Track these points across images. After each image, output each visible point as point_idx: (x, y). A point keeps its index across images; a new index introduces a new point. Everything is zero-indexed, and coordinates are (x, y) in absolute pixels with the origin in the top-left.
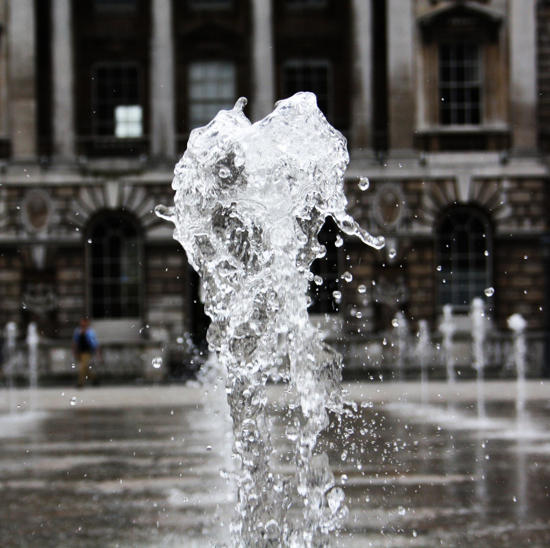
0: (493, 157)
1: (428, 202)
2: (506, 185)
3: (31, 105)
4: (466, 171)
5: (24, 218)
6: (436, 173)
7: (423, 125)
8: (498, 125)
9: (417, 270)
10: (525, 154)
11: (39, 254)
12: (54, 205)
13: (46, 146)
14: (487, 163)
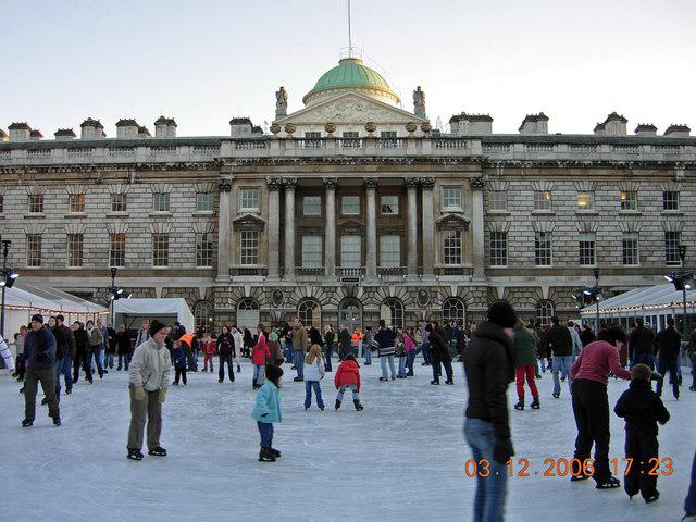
0: (467, 278)
1: (439, 296)
2: (471, 289)
7: (438, 265)
8: (469, 265)
10: (479, 276)
13: (282, 272)
14: (463, 280)
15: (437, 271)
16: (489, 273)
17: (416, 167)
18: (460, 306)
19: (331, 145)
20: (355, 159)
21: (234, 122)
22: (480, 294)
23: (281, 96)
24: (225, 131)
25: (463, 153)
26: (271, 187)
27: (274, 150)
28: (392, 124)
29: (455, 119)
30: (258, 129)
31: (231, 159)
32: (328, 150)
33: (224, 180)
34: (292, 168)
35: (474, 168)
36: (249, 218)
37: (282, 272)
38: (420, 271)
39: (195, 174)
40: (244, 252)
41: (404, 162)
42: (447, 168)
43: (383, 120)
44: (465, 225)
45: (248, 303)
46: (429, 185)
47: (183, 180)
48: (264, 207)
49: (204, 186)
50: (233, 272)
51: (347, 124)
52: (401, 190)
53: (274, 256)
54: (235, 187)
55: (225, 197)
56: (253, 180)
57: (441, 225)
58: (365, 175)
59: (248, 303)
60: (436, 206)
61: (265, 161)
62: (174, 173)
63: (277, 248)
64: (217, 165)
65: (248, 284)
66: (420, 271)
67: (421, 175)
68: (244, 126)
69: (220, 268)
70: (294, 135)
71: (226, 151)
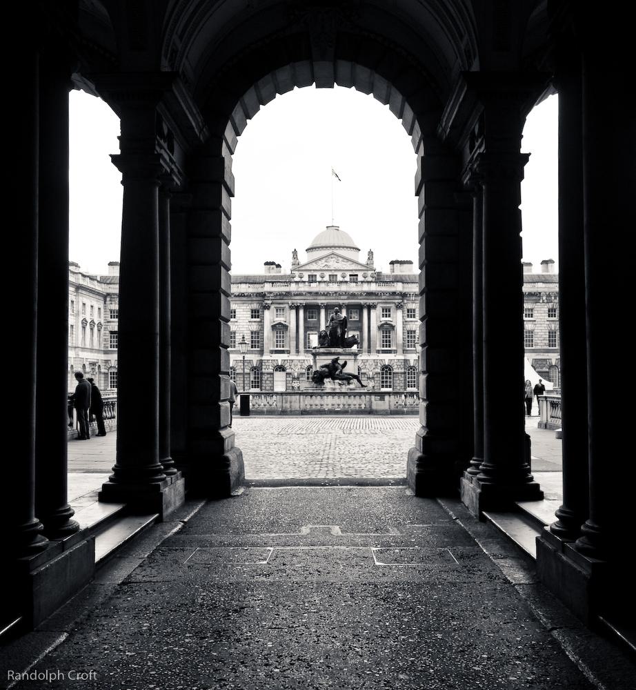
1: (379, 364)
3: (295, 342)
4: (387, 358)
5: (293, 367)
6: (381, 358)
7: (378, 348)
8: (394, 348)
9: (377, 379)
10: (400, 355)
11: (296, 375)
12: (299, 364)
13: (298, 352)
14: (391, 356)
15: (378, 352)
16: (405, 352)
17: (367, 297)
18: (390, 370)
19: (323, 285)
20: (336, 293)
21: (267, 264)
22: (398, 363)
23: (295, 252)
24: (260, 271)
25: (393, 289)
26: (291, 308)
27: (293, 288)
28: (356, 270)
29: (392, 263)
30: (279, 266)
31: (270, 293)
32: (323, 288)
33: (266, 304)
34: (302, 297)
35: (398, 297)
36: (280, 324)
37: (298, 352)
38: (369, 352)
39: (250, 299)
40: (277, 341)
41: (361, 295)
42: (383, 297)
43: (351, 269)
44: (393, 327)
45: (281, 368)
46: (374, 307)
47: (244, 302)
48: (288, 318)
49: (255, 306)
50: (272, 352)
51: (331, 270)
52: (360, 308)
53: (293, 343)
54: (272, 307)
55: (267, 313)
56: (282, 303)
57: (380, 327)
58: (341, 302)
59: (281, 368)
60: (378, 317)
61: (288, 294)
62: (237, 298)
63: (295, 339)
64: (262, 295)
65: (280, 358)
66: (369, 352)
67: (370, 302)
68: (272, 266)
69: (265, 350)
70: (304, 279)
71: (267, 288)
